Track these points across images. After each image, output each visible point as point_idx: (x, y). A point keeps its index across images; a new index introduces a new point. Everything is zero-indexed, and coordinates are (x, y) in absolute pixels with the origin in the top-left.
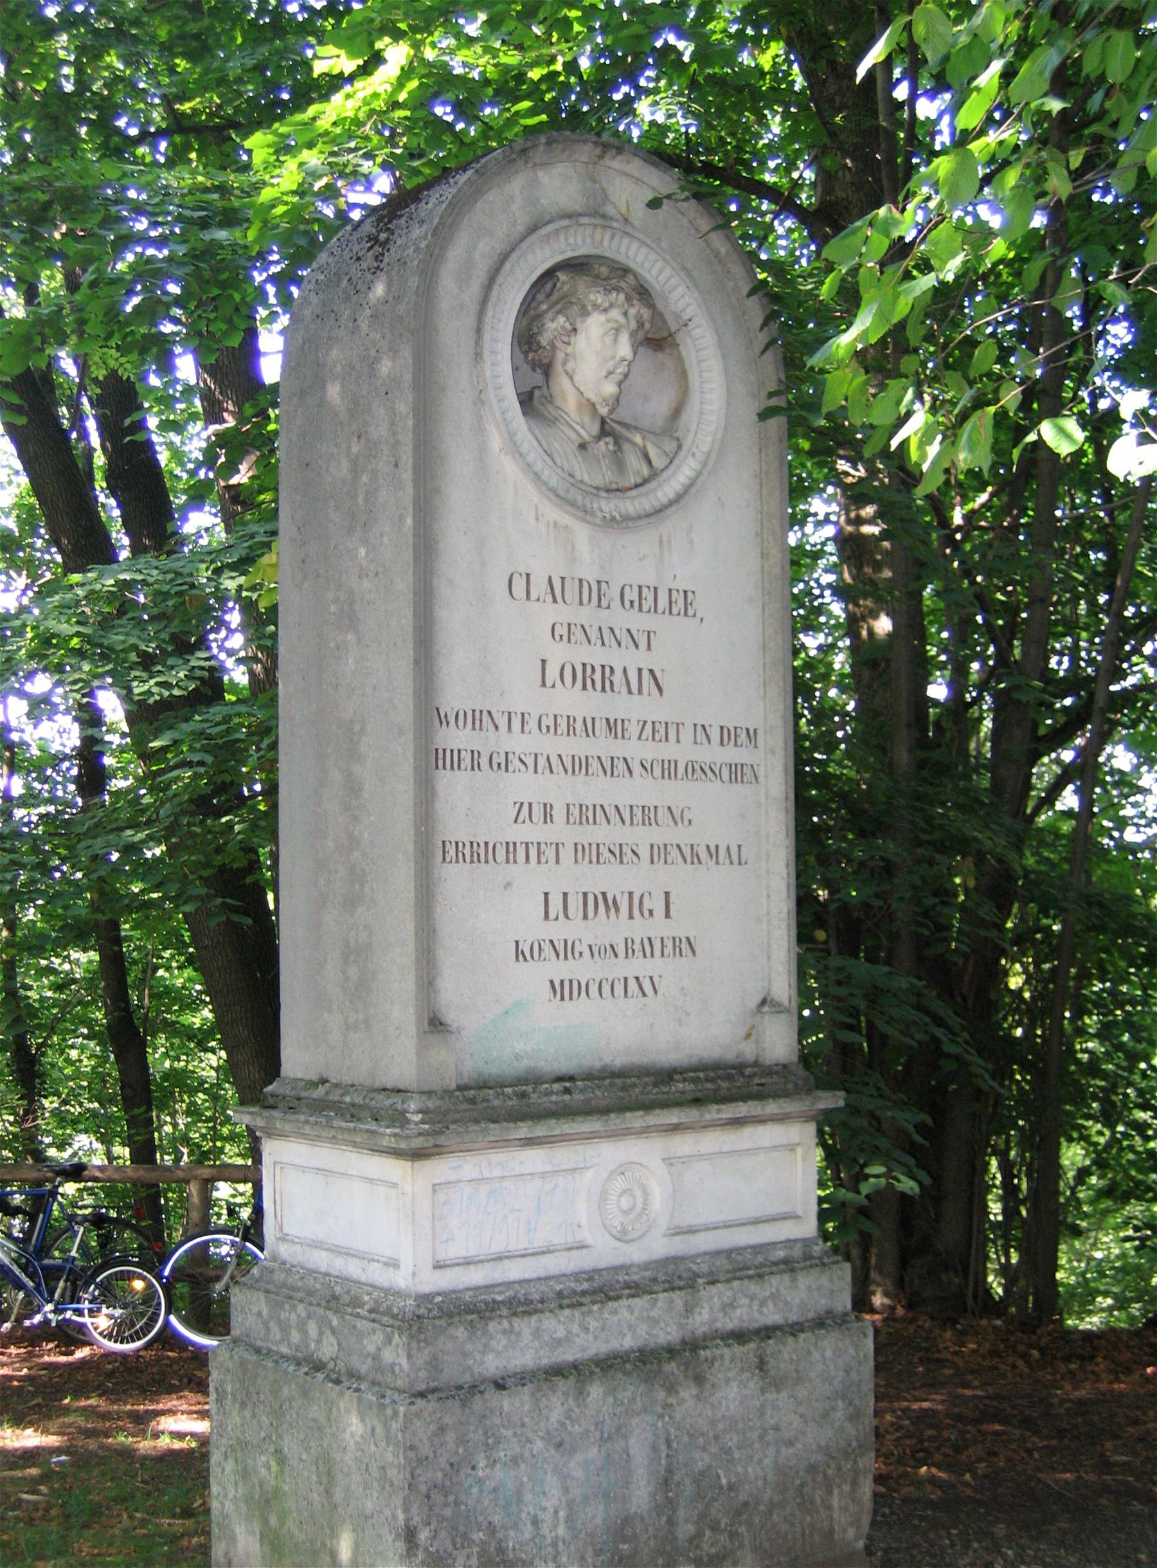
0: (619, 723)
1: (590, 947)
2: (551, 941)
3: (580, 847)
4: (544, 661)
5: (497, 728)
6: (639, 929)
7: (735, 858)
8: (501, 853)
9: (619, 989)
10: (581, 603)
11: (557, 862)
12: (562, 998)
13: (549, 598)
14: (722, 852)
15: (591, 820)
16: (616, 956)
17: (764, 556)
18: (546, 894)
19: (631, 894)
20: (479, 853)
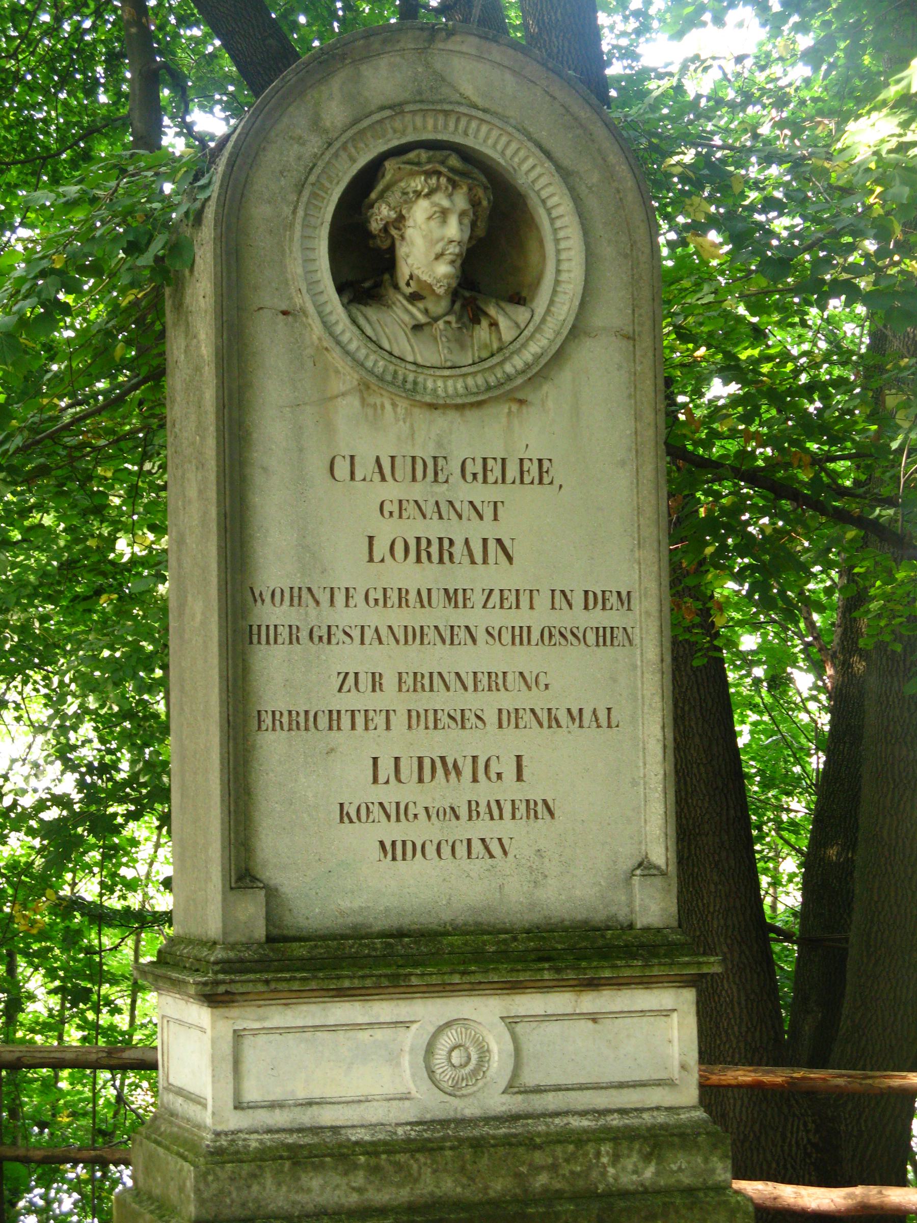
0: (460, 593)
1: (427, 809)
2: (381, 804)
3: (414, 714)
4: (371, 538)
5: (317, 603)
6: (485, 792)
7: (603, 721)
8: (323, 721)
9: (461, 850)
10: (414, 479)
11: (388, 728)
12: (394, 859)
13: (377, 477)
14: (587, 715)
15: (427, 687)
16: (457, 818)
17: (637, 417)
18: (375, 760)
19: (475, 758)
20: (301, 722)
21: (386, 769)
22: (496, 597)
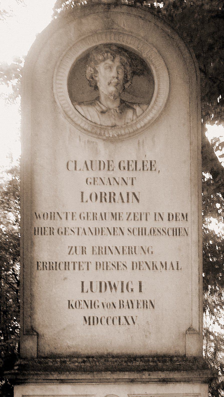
9: (116, 321)
21: (87, 286)
22: (132, 216)
